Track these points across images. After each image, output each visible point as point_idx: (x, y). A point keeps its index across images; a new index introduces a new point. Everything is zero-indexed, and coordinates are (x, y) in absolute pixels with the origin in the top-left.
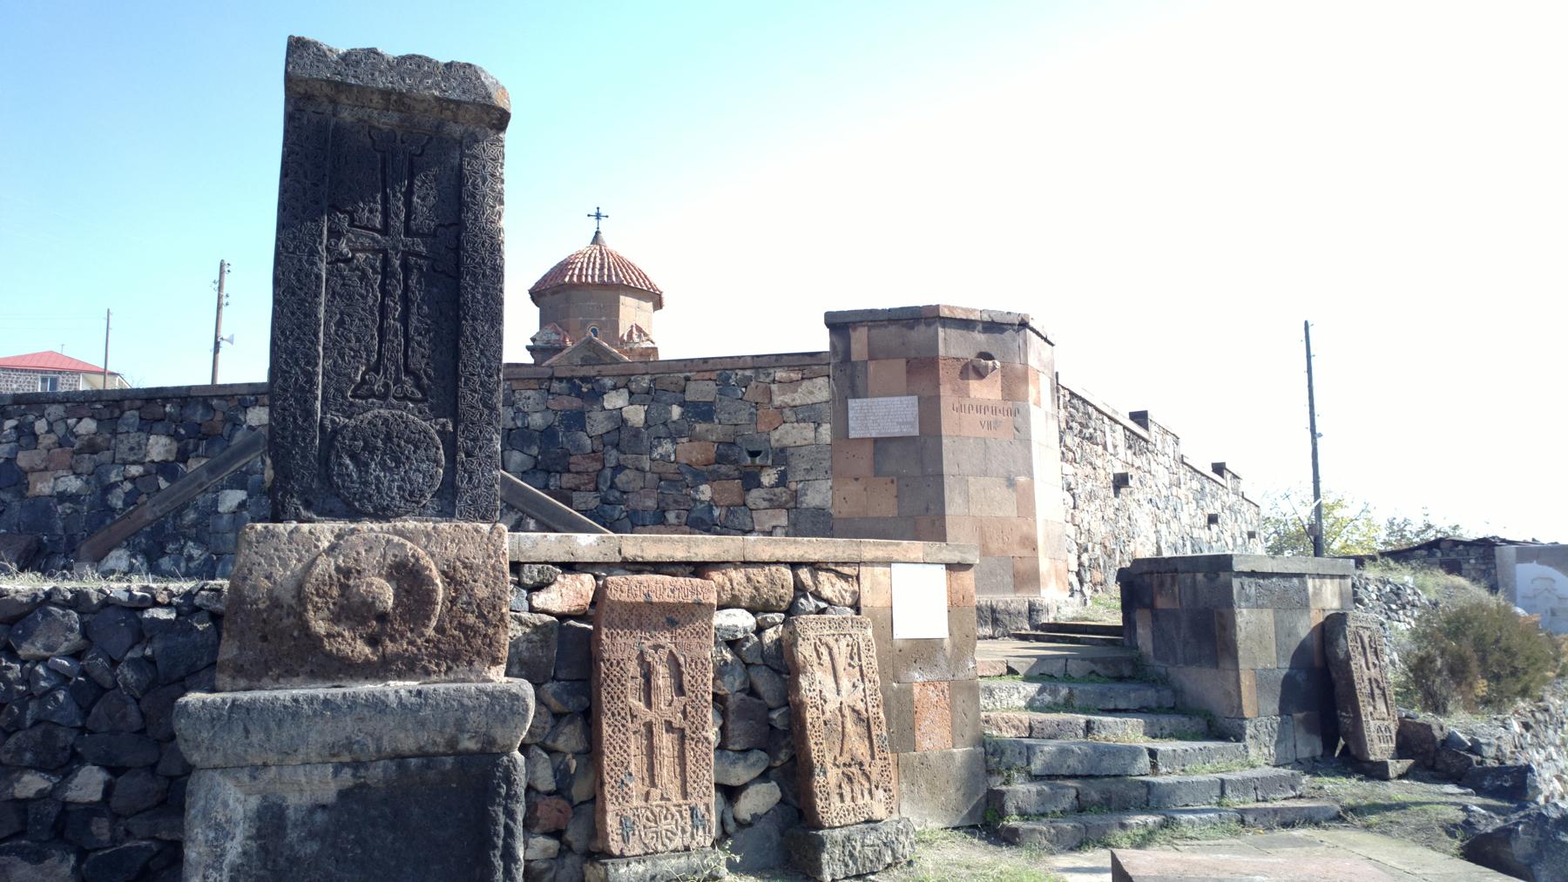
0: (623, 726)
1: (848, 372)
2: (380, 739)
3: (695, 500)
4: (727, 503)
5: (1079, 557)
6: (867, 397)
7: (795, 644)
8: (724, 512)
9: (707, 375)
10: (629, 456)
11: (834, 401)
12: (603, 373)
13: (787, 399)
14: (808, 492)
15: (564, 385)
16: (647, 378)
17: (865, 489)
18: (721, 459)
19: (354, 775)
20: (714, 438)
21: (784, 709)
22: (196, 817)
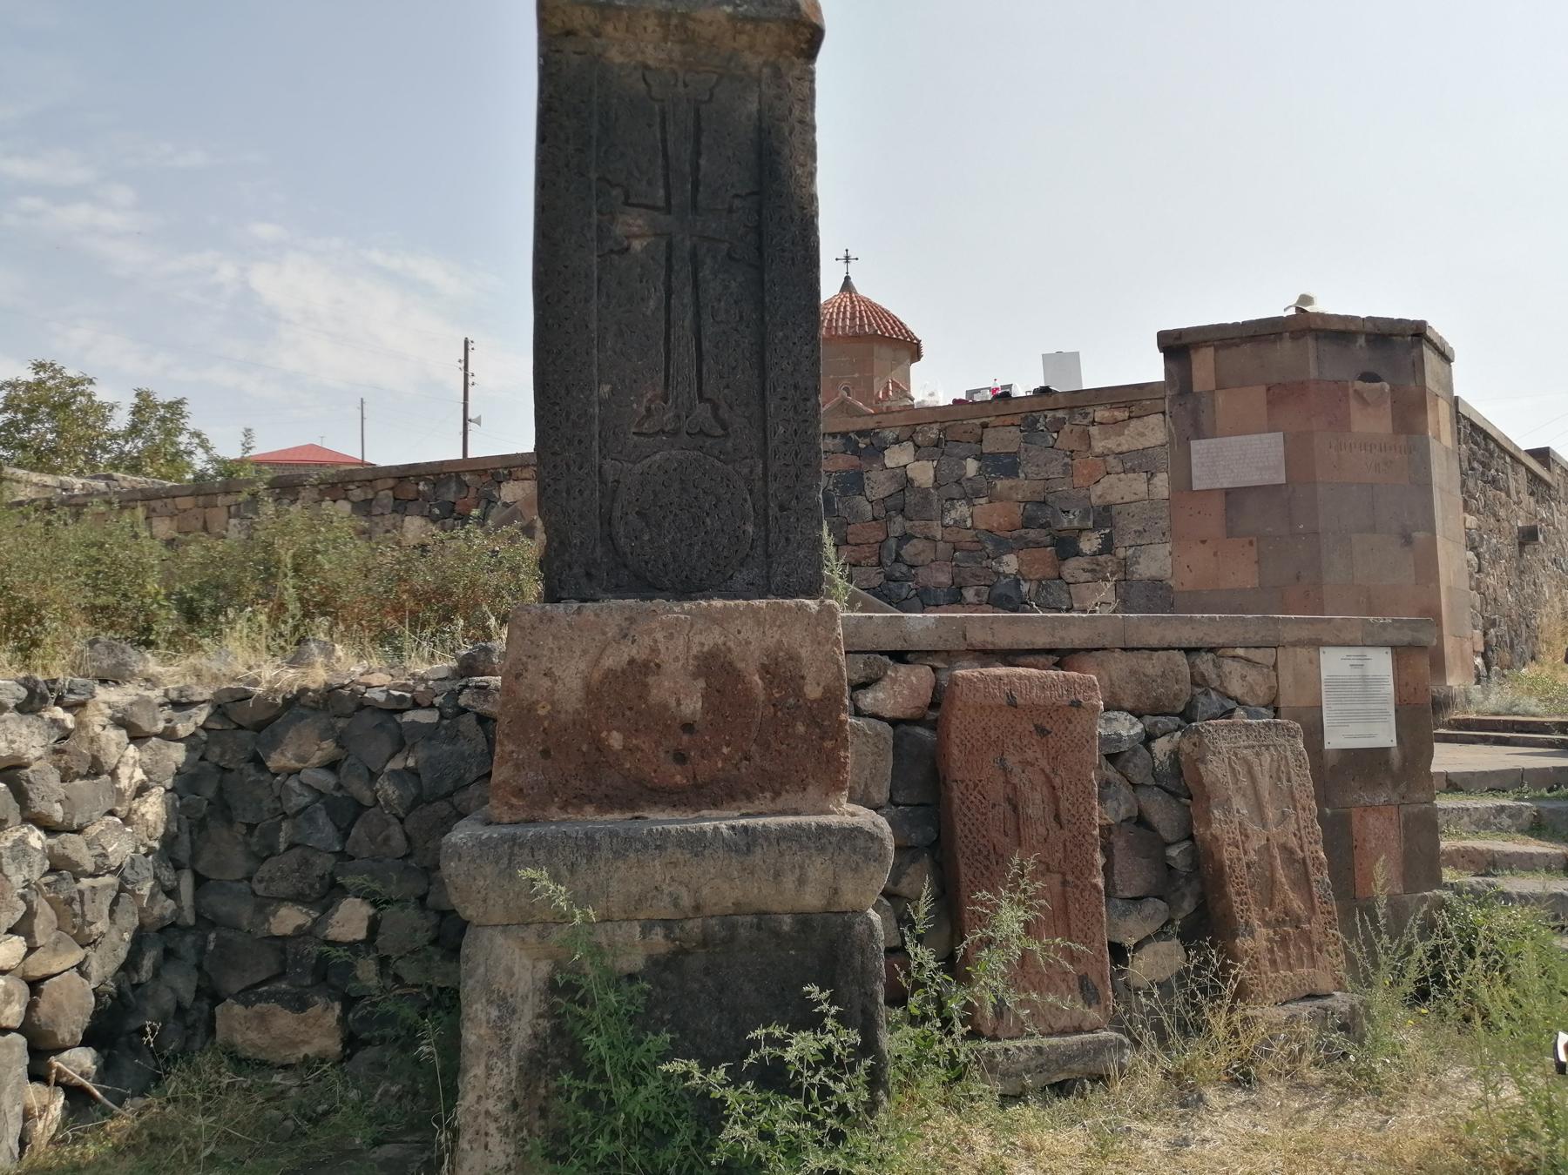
0: (987, 868)
1: (1189, 406)
3: (997, 573)
5: (1485, 634)
7: (1203, 760)
8: (1034, 586)
9: (1009, 420)
10: (917, 523)
12: (883, 425)
13: (1111, 444)
14: (1141, 560)
15: (837, 441)
16: (936, 427)
17: (1215, 554)
18: (1028, 522)
19: (666, 937)
21: (1186, 845)
22: (474, 989)
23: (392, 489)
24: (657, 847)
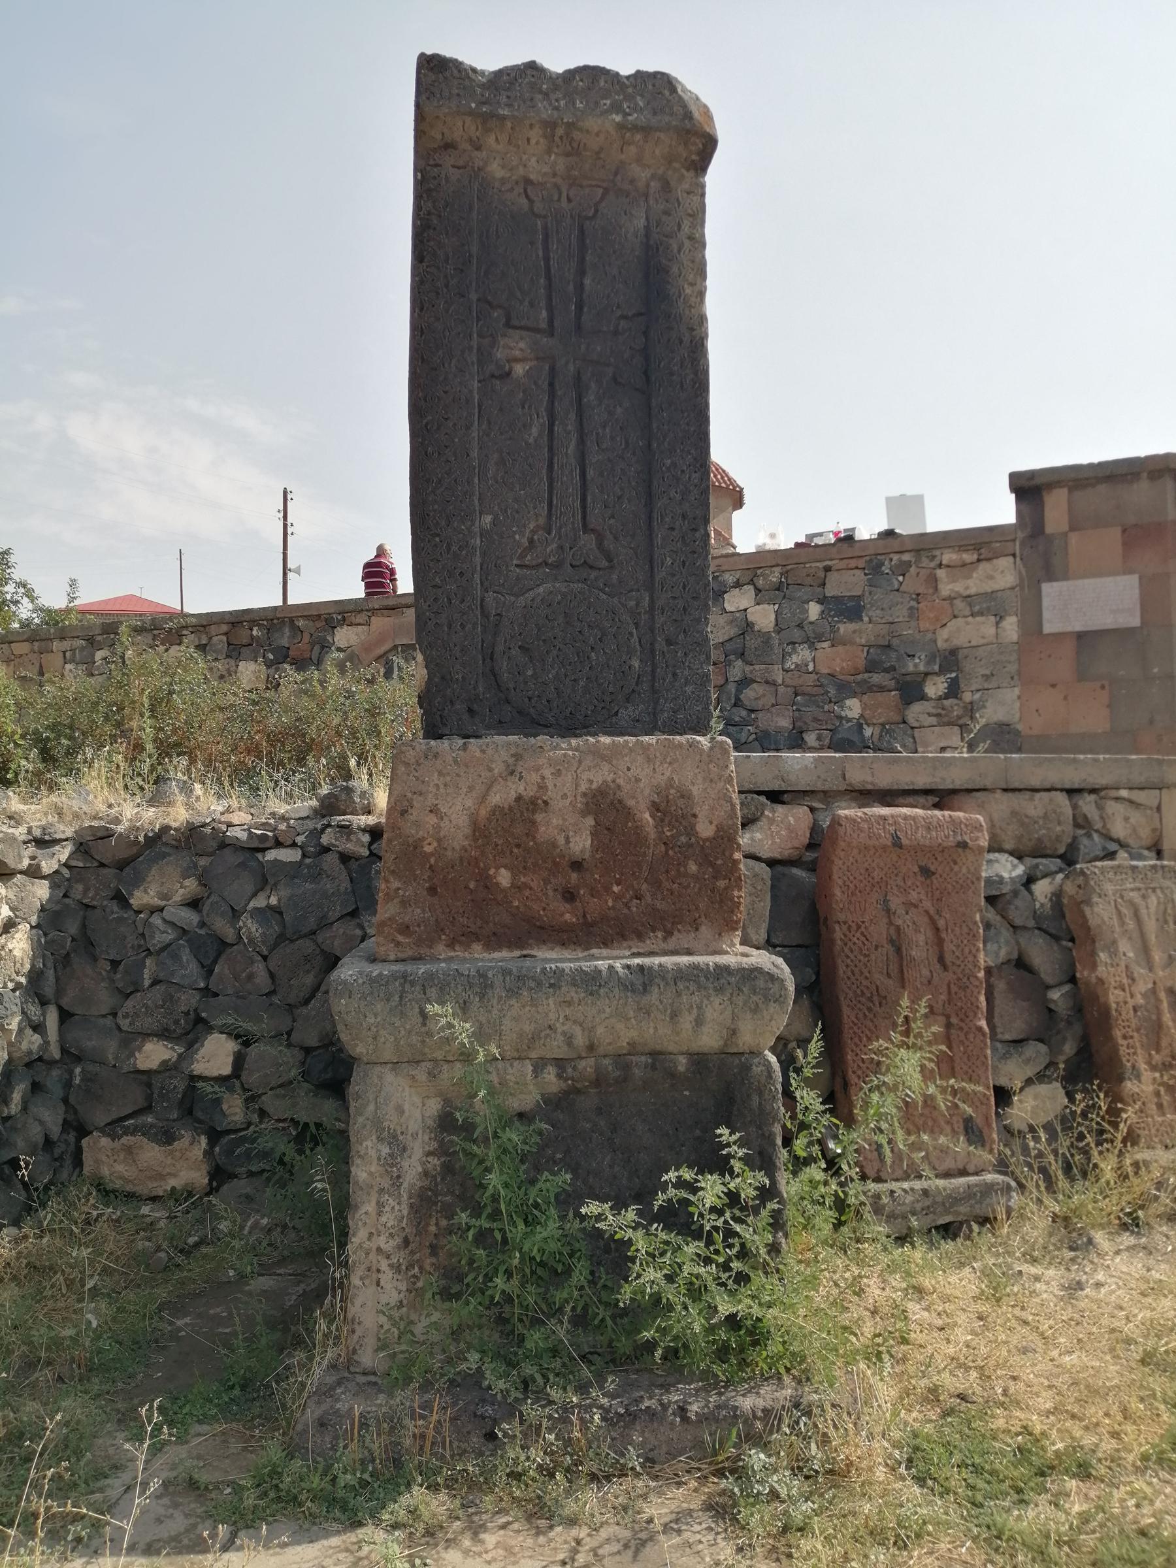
0: (870, 1009)
2: (592, 1029)
3: (840, 718)
4: (881, 721)
6: (1066, 578)
7: (1088, 902)
8: (877, 730)
9: (853, 563)
10: (757, 667)
11: (1022, 589)
12: (723, 568)
13: (959, 587)
14: (988, 704)
16: (777, 570)
17: (1065, 698)
18: (872, 666)
19: (559, 1076)
20: (863, 641)
21: (1067, 988)
23: (226, 634)
24: (551, 986)
